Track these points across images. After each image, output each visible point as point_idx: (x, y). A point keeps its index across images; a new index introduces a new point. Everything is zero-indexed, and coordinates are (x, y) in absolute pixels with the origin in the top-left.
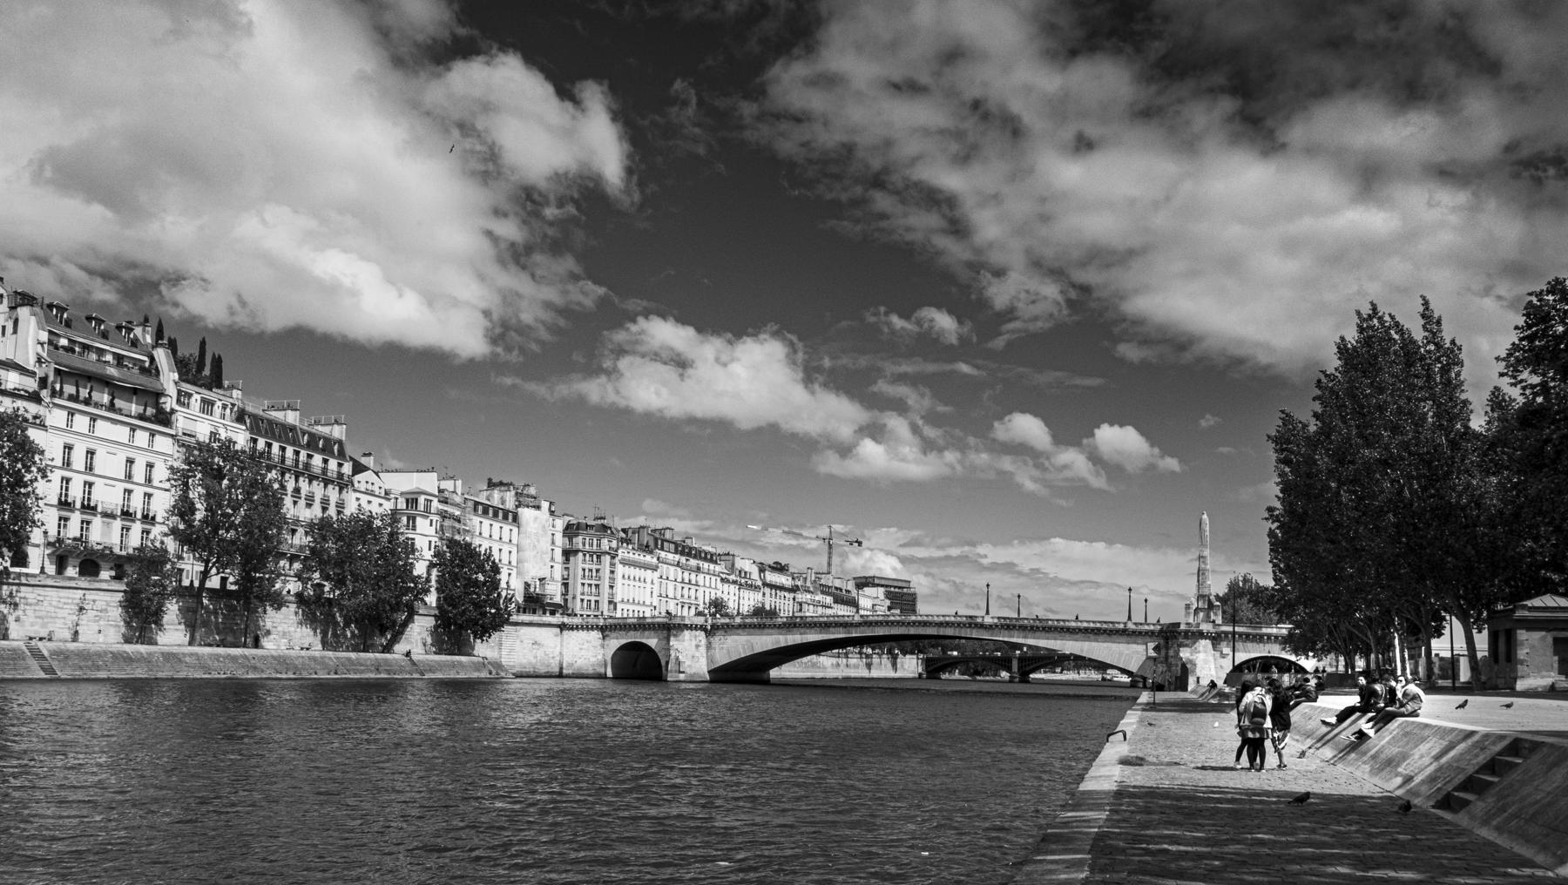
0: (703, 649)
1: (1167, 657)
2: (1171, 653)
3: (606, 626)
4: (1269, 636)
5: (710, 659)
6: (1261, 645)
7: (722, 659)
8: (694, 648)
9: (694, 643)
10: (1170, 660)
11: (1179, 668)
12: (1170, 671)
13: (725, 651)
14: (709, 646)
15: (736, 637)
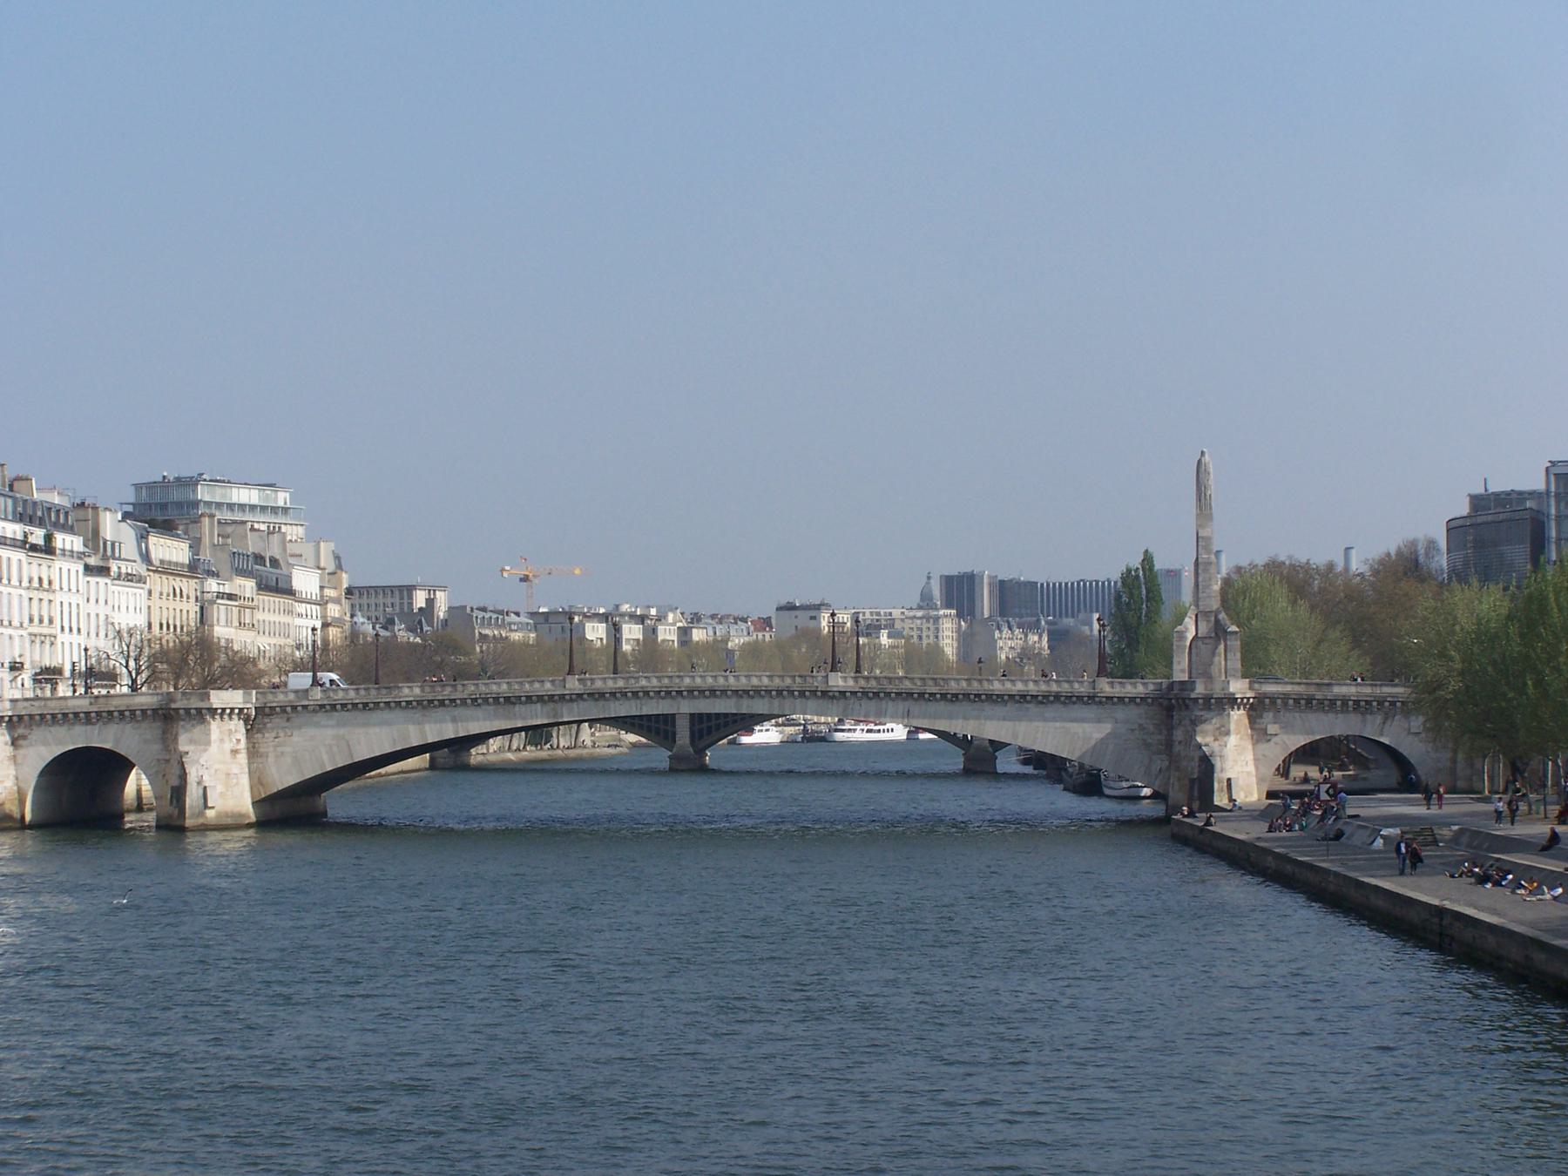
0: (243, 758)
1: (1169, 744)
2: (1179, 734)
3: (20, 717)
4: (1345, 701)
5: (256, 779)
6: (1331, 716)
7: (284, 776)
8: (228, 755)
9: (228, 746)
10: (1177, 748)
11: (1195, 763)
12: (1178, 769)
13: (289, 760)
14: (253, 753)
15: (311, 732)
